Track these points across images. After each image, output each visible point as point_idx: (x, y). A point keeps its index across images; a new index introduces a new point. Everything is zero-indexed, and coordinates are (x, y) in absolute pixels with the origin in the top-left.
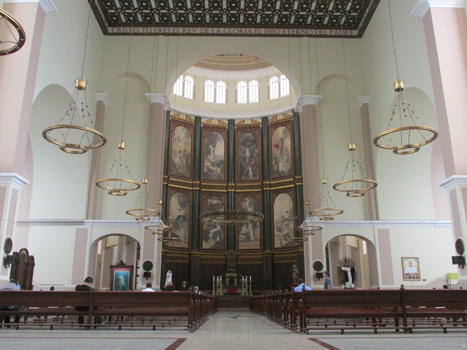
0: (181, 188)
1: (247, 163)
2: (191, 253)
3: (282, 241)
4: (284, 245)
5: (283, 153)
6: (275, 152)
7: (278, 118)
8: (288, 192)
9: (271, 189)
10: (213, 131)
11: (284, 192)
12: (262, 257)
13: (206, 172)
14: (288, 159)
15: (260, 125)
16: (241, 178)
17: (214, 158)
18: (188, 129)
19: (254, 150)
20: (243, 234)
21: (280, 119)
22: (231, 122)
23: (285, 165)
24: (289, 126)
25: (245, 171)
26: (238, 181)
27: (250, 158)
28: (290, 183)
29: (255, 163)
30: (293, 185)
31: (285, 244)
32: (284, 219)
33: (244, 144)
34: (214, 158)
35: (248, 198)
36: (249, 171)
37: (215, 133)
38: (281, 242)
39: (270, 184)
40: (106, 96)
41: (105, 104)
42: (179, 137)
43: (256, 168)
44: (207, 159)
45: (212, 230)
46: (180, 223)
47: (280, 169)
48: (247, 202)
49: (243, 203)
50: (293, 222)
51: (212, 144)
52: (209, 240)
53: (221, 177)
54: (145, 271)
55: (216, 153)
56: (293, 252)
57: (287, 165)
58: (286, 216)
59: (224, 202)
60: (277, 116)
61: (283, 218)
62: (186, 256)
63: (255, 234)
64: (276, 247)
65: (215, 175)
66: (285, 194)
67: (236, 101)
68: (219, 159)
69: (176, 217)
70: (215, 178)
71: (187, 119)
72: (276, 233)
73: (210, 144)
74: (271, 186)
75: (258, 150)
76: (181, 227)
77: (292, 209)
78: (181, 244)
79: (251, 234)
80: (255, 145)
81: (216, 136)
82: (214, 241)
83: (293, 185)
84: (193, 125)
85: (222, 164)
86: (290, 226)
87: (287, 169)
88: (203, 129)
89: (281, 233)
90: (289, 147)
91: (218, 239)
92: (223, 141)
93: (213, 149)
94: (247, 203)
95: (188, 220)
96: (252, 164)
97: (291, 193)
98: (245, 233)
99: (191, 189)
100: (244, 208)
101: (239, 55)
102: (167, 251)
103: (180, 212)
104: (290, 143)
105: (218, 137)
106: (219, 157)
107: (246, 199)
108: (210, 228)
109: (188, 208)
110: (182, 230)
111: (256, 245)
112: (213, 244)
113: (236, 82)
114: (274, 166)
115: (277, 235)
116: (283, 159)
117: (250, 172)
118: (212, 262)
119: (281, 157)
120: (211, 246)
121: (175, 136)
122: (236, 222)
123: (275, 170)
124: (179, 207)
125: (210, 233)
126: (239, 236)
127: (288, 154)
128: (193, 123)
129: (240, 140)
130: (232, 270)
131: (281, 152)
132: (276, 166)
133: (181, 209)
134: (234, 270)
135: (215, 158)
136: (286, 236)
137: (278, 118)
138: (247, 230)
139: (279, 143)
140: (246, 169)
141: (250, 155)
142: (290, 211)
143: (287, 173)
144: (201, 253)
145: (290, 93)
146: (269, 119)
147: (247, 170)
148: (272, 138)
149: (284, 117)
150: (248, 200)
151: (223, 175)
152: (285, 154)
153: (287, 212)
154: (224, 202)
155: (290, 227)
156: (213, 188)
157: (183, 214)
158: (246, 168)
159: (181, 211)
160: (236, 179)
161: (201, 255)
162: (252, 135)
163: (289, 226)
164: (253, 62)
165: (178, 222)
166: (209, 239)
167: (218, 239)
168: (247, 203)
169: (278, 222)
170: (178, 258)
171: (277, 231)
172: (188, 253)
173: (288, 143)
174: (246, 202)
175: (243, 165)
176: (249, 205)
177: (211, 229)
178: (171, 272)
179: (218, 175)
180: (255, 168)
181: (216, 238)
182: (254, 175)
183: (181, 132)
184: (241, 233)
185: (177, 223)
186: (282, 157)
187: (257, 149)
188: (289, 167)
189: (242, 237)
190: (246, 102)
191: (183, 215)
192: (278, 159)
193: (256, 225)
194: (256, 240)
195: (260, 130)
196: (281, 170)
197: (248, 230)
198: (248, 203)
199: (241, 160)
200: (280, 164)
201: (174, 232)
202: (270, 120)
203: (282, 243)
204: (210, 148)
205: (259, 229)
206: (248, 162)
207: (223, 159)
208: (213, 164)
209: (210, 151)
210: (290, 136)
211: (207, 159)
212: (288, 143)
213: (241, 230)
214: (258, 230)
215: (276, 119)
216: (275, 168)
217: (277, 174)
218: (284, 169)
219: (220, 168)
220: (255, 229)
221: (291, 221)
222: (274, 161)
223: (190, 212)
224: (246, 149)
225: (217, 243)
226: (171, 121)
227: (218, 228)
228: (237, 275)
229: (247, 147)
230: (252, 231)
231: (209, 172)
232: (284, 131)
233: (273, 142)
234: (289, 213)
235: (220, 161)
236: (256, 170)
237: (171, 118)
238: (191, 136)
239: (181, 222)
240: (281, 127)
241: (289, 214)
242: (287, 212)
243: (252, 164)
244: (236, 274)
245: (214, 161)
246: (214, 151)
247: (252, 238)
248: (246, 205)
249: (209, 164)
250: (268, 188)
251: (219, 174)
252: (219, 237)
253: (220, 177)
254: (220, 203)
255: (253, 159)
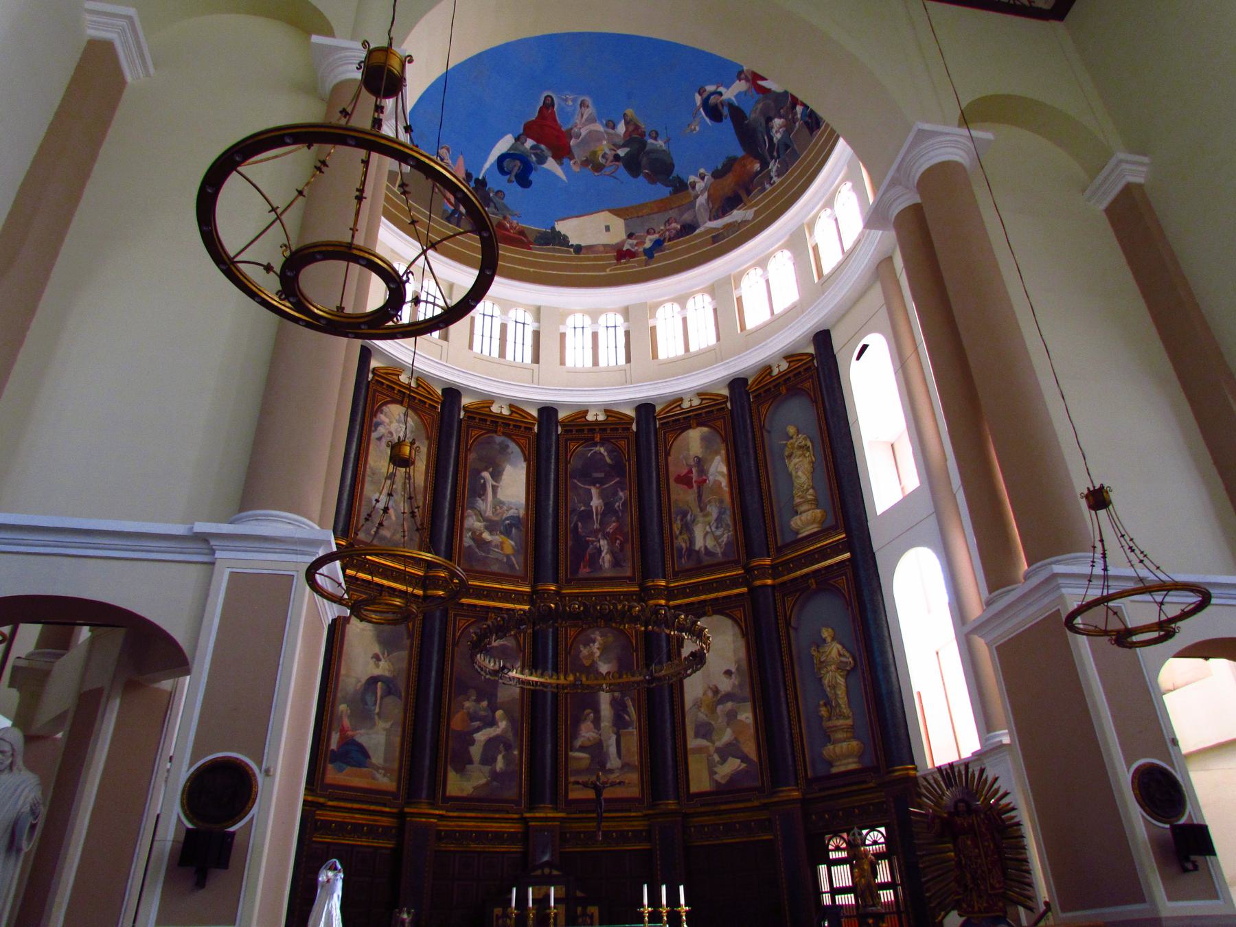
0: (389, 587)
1: (595, 527)
2: (407, 810)
3: (715, 769)
4: (723, 782)
5: (703, 497)
6: (682, 496)
7: (686, 405)
8: (727, 611)
9: (672, 603)
10: (496, 432)
11: (716, 612)
12: (646, 828)
13: (470, 546)
14: (721, 514)
15: (631, 424)
16: (575, 570)
17: (494, 507)
18: (420, 416)
19: (616, 494)
20: (582, 749)
21: (691, 406)
22: (548, 412)
23: (712, 533)
24: (720, 423)
25: (590, 549)
26: (568, 581)
27: (604, 514)
28: (734, 582)
29: (618, 530)
30: (744, 590)
31: (727, 778)
32: (720, 695)
33: (585, 474)
34: (496, 510)
35: (597, 633)
36: (600, 551)
37: (499, 439)
38: (712, 773)
39: (666, 587)
40: (130, 18)
41: (129, 78)
42: (391, 433)
43: (621, 544)
44: (473, 508)
45: (480, 733)
46: (375, 704)
47: (699, 544)
48: (597, 645)
49: (582, 649)
50: (749, 705)
51: (491, 469)
52: (469, 767)
53: (514, 565)
54: (190, 826)
55: (500, 496)
56: (756, 803)
57: (718, 533)
58: (726, 685)
59: (522, 642)
60: (681, 399)
61: (716, 691)
62: (385, 821)
63: (622, 745)
64: (694, 788)
65: (497, 559)
66: (716, 618)
67: (562, 362)
68: (511, 513)
69: (363, 680)
70: (495, 568)
71: (420, 388)
72: (693, 742)
73: (486, 469)
74: (670, 594)
75: (627, 492)
76: (376, 717)
77: (744, 664)
78: (374, 778)
79: (608, 746)
80: (618, 479)
81: (504, 449)
82: (487, 769)
83: (744, 590)
84: (436, 408)
85: (518, 528)
86: (739, 717)
87: (720, 544)
88: (464, 425)
89: (713, 742)
90: (724, 483)
91: (500, 764)
92: (524, 465)
93: (494, 483)
94: (595, 648)
95: (403, 694)
96: (608, 533)
97: (739, 614)
98: (590, 744)
99: (420, 592)
100: (587, 663)
101: (572, 250)
102: (322, 800)
103: (377, 666)
104: (724, 469)
105: (510, 450)
106: (511, 508)
107: (593, 636)
108: (477, 724)
109: (404, 654)
110: (382, 725)
111: (631, 785)
112: (483, 781)
113: (563, 315)
114: (677, 538)
115: (699, 750)
116: (706, 516)
117: (603, 554)
118: (478, 847)
119: (698, 510)
120: (475, 788)
121: (381, 430)
122: (588, 683)
123: (681, 547)
124: (376, 649)
125: (473, 742)
126: (571, 754)
127: (721, 501)
128: (437, 402)
129: (575, 463)
130: (550, 875)
131: (700, 496)
132: (685, 537)
133: (383, 654)
134: (555, 872)
135: (498, 508)
136: (726, 752)
137: (686, 405)
138: (594, 735)
139: (690, 471)
140: (591, 546)
141: (602, 504)
142: (737, 669)
143: (720, 555)
144: (441, 812)
145: (718, 339)
146: (658, 409)
147: (596, 548)
148: (670, 459)
149: (704, 402)
150: (599, 638)
151: (521, 558)
152: (710, 502)
153: (728, 673)
154: (522, 642)
155: (741, 721)
156: (487, 597)
157: (387, 674)
158: (594, 541)
159: (382, 663)
160: (562, 574)
161: (441, 817)
162: (610, 452)
163: (736, 717)
164: (608, 270)
165: (369, 699)
166: (471, 762)
167: (500, 764)
168: (595, 648)
169: (698, 704)
170: (357, 829)
171: (697, 735)
172: (394, 810)
173: (719, 470)
174: (591, 645)
175: (584, 534)
176: (601, 654)
177: (478, 729)
178: (339, 866)
179: (505, 560)
180: (618, 541)
181: (494, 760)
182: (616, 563)
183: (399, 422)
184: (578, 743)
185: (366, 704)
186: (702, 510)
187: (622, 490)
188: (726, 536)
189: (580, 759)
190: (589, 363)
191: (387, 677)
192: (689, 517)
193: (627, 717)
194: (625, 766)
195: (633, 438)
196: (701, 548)
197: (600, 735)
198: (598, 649)
199: (575, 518)
200: (699, 532)
201: (350, 733)
202: (663, 410)
203: (717, 777)
204: (483, 478)
205: (635, 732)
206: (596, 526)
207: (522, 512)
208: (491, 526)
209: (484, 486)
210: (723, 452)
211: (473, 508)
212: (718, 469)
213: (575, 734)
214: (631, 733)
215: (678, 408)
216: (681, 542)
217: (688, 559)
218: (710, 543)
219: (512, 540)
220: (622, 731)
221: (744, 700)
222: (679, 522)
223: (409, 670)
224: (589, 491)
225: (495, 776)
226: (371, 385)
227: (503, 724)
228: (567, 890)
229: (594, 485)
230: (614, 737)
231: (478, 547)
232: (704, 439)
233: (671, 469)
234: (733, 676)
235: (512, 518)
236: (622, 550)
237: (371, 376)
238: (428, 438)
239: (378, 702)
240: (694, 428)
241: (735, 680)
242: (728, 673)
243: (611, 531)
244: (564, 889)
245: (496, 519)
246: (494, 489)
247: (614, 762)
248: (592, 654)
249: (480, 524)
250: (663, 599)
251: (508, 556)
252: (504, 757)
253: (512, 566)
254: (509, 644)
255: (614, 518)
